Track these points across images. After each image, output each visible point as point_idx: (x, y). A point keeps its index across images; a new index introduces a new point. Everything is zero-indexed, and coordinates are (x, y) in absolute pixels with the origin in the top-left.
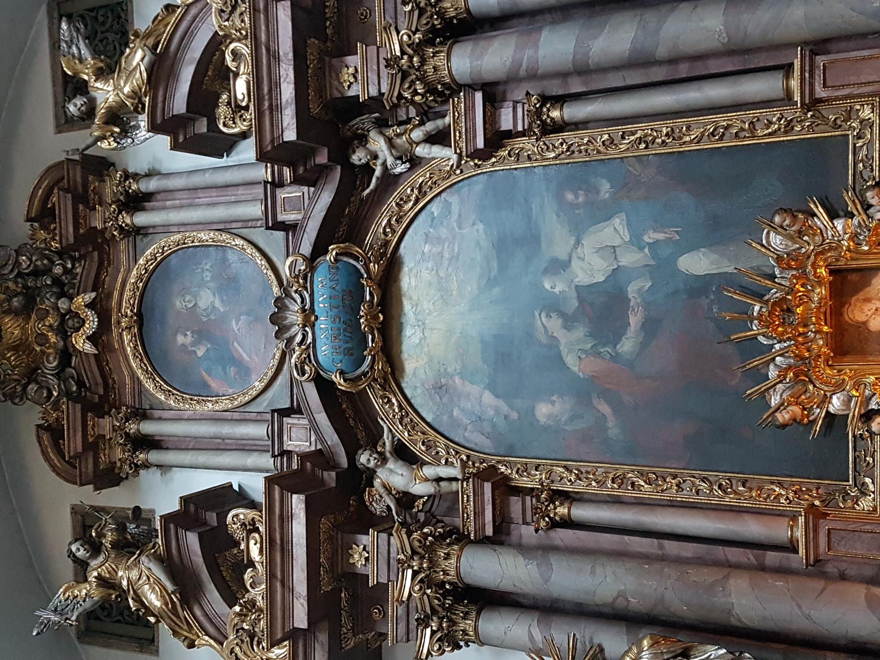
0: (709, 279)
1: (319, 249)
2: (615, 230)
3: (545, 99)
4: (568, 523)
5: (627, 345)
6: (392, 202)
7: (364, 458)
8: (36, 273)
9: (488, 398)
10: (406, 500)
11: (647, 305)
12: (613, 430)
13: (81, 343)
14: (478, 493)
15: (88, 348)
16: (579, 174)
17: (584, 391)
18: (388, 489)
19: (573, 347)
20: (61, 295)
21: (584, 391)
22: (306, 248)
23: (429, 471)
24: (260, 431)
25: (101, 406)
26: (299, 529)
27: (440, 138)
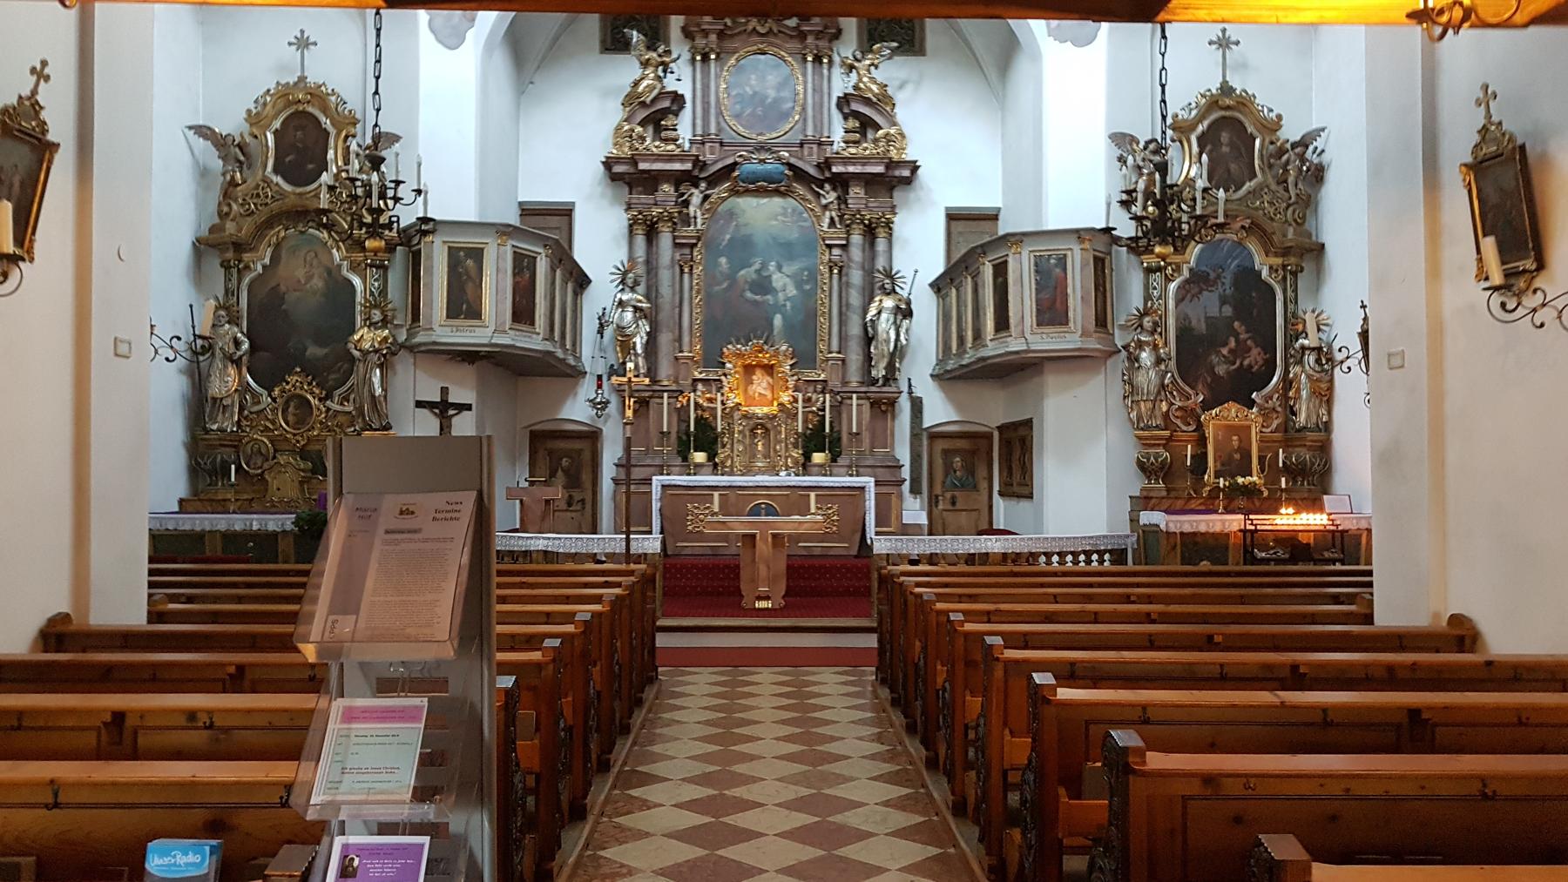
0: (771, 325)
1: (791, 166)
2: (792, 291)
4: (682, 272)
5: (749, 295)
6: (809, 197)
7: (703, 185)
10: (686, 204)
17: (731, 277)
21: (731, 277)
22: (792, 161)
23: (699, 213)
24: (713, 130)
25: (721, 35)
26: (677, 166)
27: (832, 223)
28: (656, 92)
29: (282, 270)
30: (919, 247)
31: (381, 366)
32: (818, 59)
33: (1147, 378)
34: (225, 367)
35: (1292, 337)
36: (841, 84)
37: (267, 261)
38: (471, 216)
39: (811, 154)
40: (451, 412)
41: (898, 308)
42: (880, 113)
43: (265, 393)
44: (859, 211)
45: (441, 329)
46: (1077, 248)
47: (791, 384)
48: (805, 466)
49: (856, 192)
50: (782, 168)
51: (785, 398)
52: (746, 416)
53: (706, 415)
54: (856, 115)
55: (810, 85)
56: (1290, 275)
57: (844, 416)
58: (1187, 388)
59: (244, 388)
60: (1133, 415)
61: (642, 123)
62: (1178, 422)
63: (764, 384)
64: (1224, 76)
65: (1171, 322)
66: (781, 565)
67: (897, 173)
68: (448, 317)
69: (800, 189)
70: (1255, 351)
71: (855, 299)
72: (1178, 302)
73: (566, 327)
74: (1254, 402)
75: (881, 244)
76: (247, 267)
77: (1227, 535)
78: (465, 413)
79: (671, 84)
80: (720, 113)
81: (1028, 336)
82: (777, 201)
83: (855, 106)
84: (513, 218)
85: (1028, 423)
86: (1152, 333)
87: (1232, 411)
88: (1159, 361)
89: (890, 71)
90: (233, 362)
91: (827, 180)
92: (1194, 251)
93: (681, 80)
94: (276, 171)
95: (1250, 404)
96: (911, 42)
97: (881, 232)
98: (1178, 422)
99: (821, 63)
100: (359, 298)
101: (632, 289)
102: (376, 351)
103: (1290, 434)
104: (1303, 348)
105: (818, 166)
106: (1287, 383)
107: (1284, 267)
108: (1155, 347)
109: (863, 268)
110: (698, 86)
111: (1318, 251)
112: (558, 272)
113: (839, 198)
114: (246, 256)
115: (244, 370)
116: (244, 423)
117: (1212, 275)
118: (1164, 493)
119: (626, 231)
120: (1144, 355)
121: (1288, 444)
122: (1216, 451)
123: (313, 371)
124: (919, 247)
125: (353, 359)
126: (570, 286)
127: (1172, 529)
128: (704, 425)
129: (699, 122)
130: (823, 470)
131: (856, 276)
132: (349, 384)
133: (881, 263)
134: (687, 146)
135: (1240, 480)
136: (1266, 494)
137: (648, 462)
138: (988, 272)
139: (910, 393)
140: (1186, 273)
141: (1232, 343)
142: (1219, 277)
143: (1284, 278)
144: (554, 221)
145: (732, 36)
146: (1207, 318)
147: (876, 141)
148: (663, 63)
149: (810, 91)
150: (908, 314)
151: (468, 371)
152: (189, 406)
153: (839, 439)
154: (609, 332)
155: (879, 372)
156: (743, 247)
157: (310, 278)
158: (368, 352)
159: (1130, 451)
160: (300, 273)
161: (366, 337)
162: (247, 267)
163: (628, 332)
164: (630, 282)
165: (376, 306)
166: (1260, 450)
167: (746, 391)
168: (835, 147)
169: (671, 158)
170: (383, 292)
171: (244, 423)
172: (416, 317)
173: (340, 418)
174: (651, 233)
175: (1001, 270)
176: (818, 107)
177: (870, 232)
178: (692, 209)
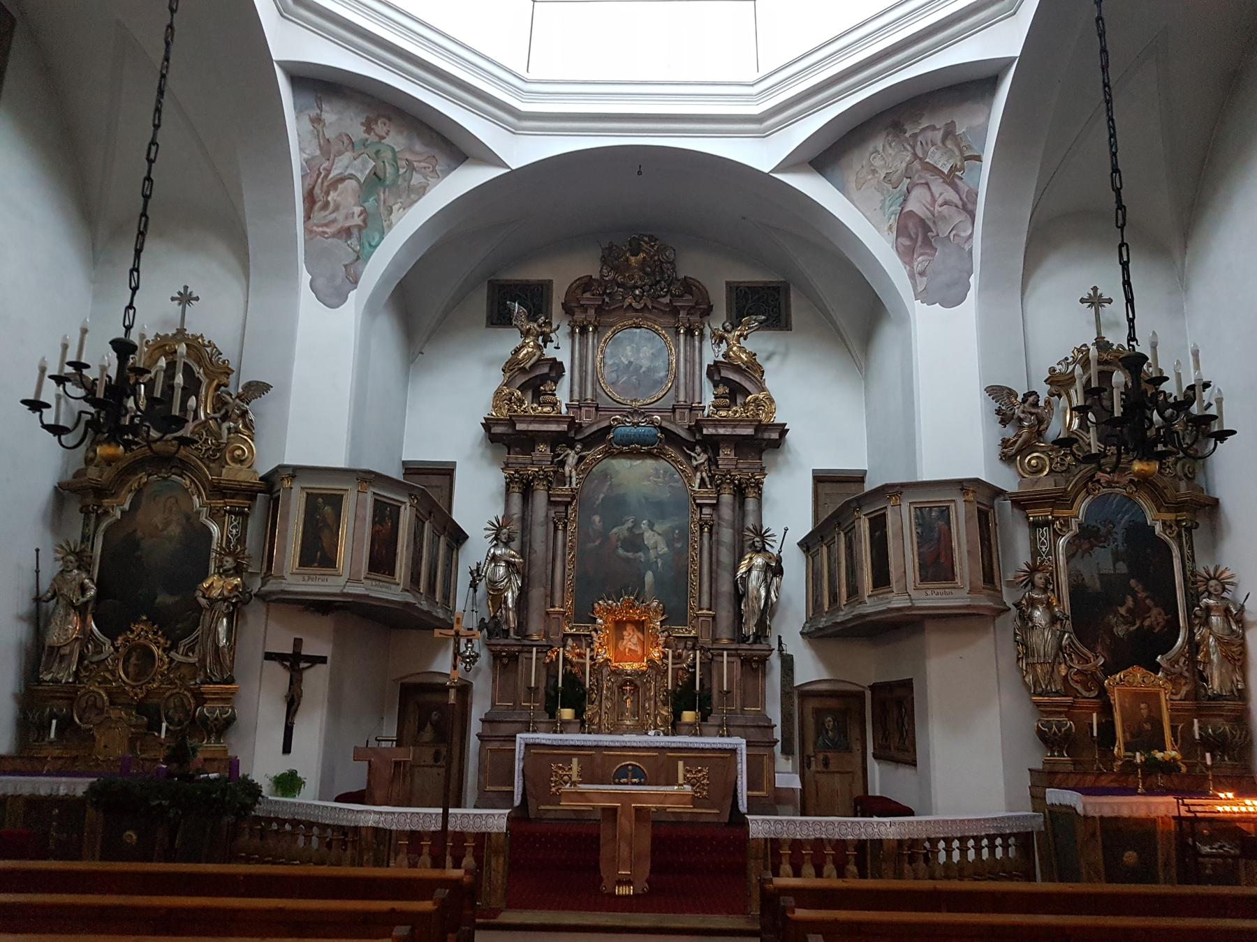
3: (712, 526)
4: (556, 529)
5: (620, 551)
8: (662, 272)
9: (602, 496)
10: (562, 464)
11: (635, 559)
12: (591, 545)
13: (629, 300)
14: (566, 496)
15: (626, 304)
16: (684, 534)
18: (567, 455)
19: (620, 531)
20: (651, 286)
22: (664, 424)
23: (574, 473)
24: (589, 396)
25: (600, 310)
26: (553, 427)
28: (535, 359)
29: (140, 516)
30: (788, 508)
31: (230, 617)
32: (690, 332)
33: (1043, 639)
35: (1193, 598)
36: (711, 353)
37: (126, 506)
38: (341, 463)
39: (682, 418)
40: (303, 665)
41: (768, 565)
42: (751, 381)
43: (108, 642)
44: (729, 471)
45: (295, 579)
46: (960, 501)
47: (661, 640)
48: (675, 726)
49: (726, 455)
50: (654, 431)
51: (656, 654)
52: (616, 673)
53: (575, 670)
54: (726, 382)
55: (682, 355)
56: (1185, 532)
57: (715, 673)
58: (1085, 650)
59: (87, 636)
60: (1029, 679)
61: (522, 388)
62: (1079, 687)
63: (635, 640)
64: (1099, 333)
65: (1063, 578)
66: (645, 843)
67: (766, 436)
68: (302, 564)
69: (671, 451)
70: (1155, 611)
71: (725, 556)
72: (1069, 558)
73: (440, 582)
74: (1159, 666)
75: (751, 504)
76: (106, 513)
77: (1154, 821)
78: (319, 667)
79: (549, 352)
80: (596, 381)
81: (909, 592)
82: (650, 463)
83: (726, 373)
84: (396, 473)
85: (907, 685)
86: (1045, 590)
87: (1137, 674)
88: (1054, 620)
89: (758, 343)
90: (75, 608)
91: (697, 443)
92: (1082, 507)
93: (561, 350)
95: (1156, 668)
96: (778, 319)
97: (751, 493)
98: (1079, 687)
99: (693, 336)
100: (214, 546)
101: (506, 545)
102: (225, 599)
103: (1201, 702)
104: (1208, 609)
105: (690, 428)
106: (1194, 646)
107: (1178, 522)
108: (1049, 606)
109: (733, 528)
110: (577, 355)
111: (1213, 506)
112: (427, 524)
113: (709, 459)
114: (106, 502)
117: (1103, 530)
118: (1071, 768)
119: (503, 489)
120: (1037, 613)
121: (1200, 712)
122: (1123, 721)
123: (161, 620)
124: (788, 508)
125: (200, 608)
126: (443, 541)
127: (1091, 813)
128: (573, 681)
129: (576, 388)
130: (694, 730)
131: (726, 534)
133: (750, 522)
134: (564, 410)
135: (1159, 755)
136: (1184, 769)
137: (515, 718)
138: (864, 526)
139: (781, 650)
140: (1075, 527)
141: (1130, 602)
142: (1109, 533)
143: (1179, 535)
144: (435, 480)
145: (610, 312)
146: (1101, 576)
147: (745, 405)
148: (543, 333)
149: (682, 360)
150: (779, 571)
151: (326, 623)
152: (27, 654)
153: (710, 698)
154: (482, 586)
155: (750, 629)
156: (617, 505)
157: (167, 524)
158: (217, 600)
159: (1027, 723)
160: (158, 520)
161: (216, 584)
162: (106, 513)
163: (500, 586)
164: (503, 538)
165: (230, 554)
166: (1172, 719)
167: (616, 647)
168: (706, 412)
169: (547, 419)
170: (241, 540)
172: (269, 567)
173: (184, 670)
174: (527, 493)
175: (878, 523)
176: (690, 375)
177: (740, 493)
178: (567, 469)
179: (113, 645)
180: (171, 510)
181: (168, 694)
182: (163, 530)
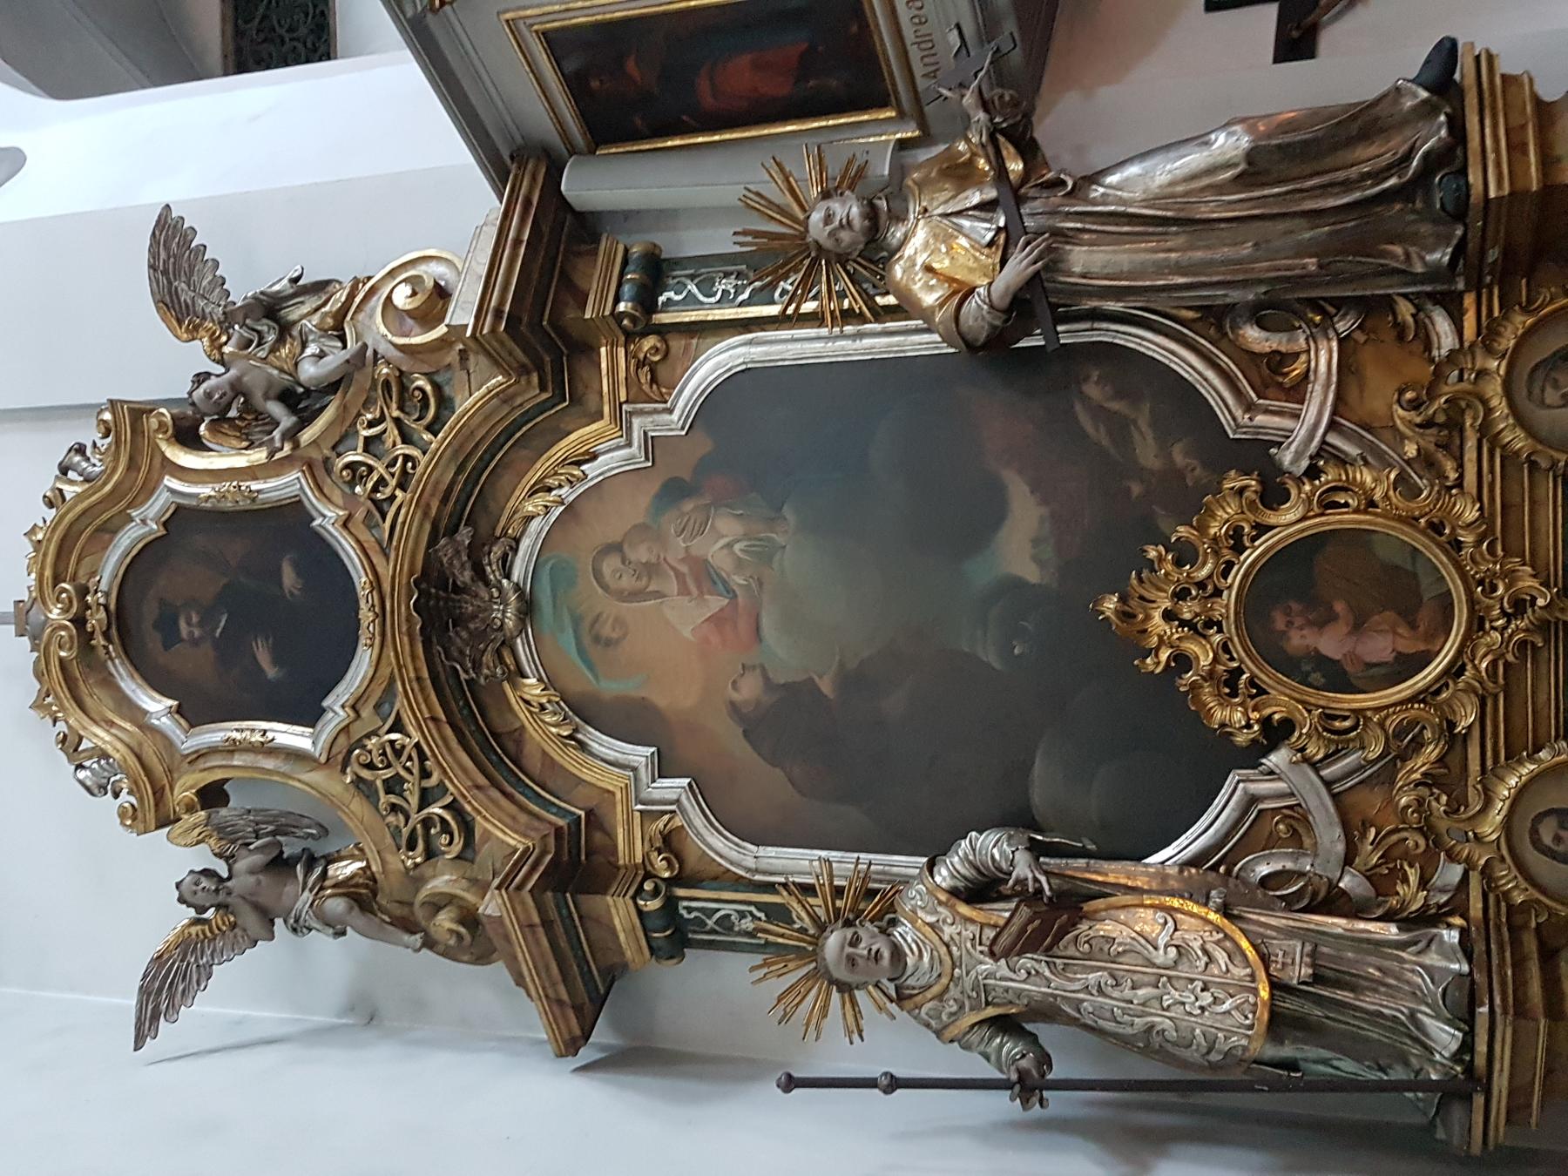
29: (676, 695)
34: (1102, 952)
94: (309, 715)
115: (1114, 872)
116: (1409, 893)
132: (1185, 363)
157: (704, 576)
160: (685, 616)
162: (670, 843)
171: (1409, 893)
179: (1252, 756)
180: (651, 570)
181: (1517, 440)
182: (730, 592)
